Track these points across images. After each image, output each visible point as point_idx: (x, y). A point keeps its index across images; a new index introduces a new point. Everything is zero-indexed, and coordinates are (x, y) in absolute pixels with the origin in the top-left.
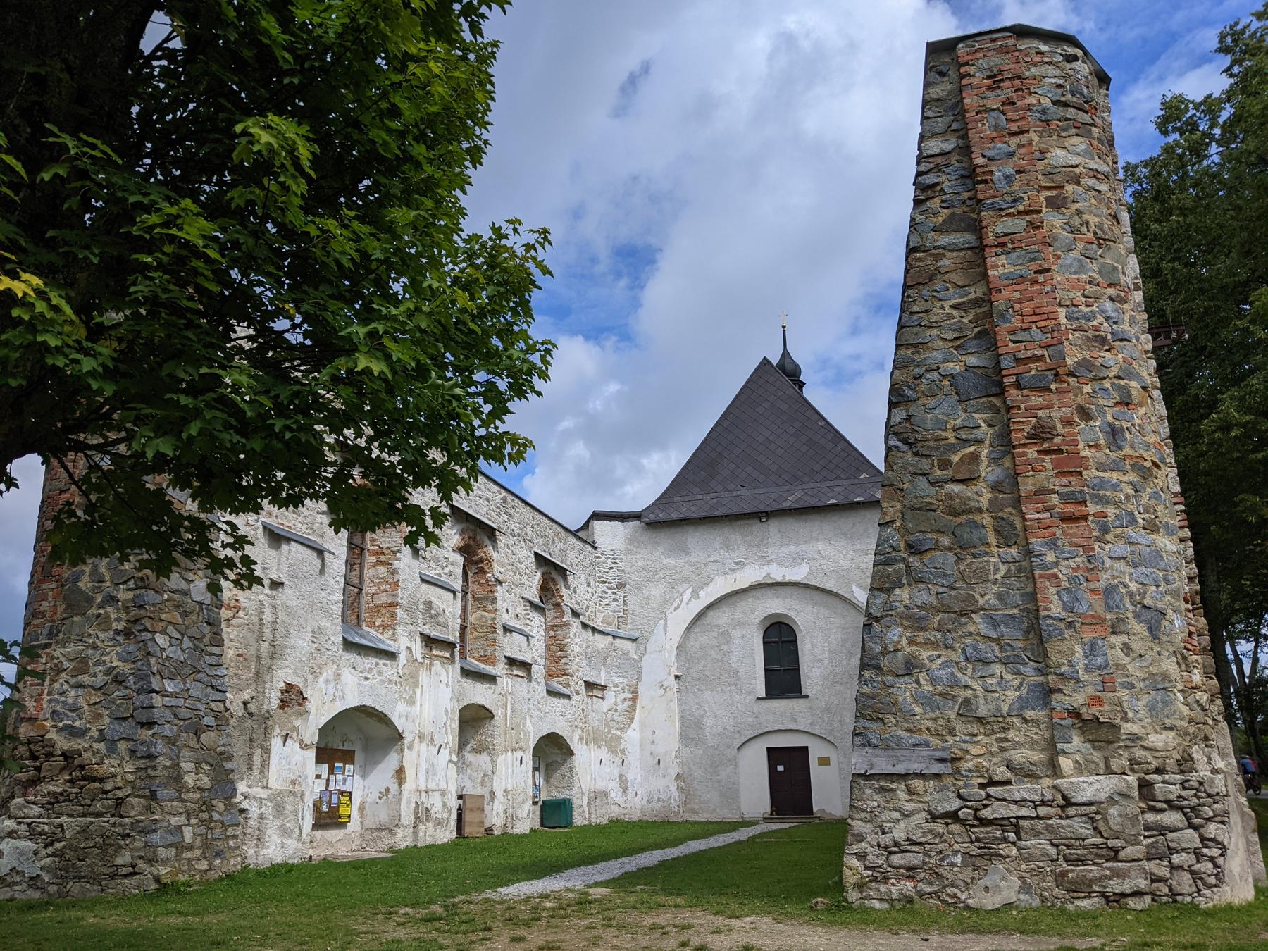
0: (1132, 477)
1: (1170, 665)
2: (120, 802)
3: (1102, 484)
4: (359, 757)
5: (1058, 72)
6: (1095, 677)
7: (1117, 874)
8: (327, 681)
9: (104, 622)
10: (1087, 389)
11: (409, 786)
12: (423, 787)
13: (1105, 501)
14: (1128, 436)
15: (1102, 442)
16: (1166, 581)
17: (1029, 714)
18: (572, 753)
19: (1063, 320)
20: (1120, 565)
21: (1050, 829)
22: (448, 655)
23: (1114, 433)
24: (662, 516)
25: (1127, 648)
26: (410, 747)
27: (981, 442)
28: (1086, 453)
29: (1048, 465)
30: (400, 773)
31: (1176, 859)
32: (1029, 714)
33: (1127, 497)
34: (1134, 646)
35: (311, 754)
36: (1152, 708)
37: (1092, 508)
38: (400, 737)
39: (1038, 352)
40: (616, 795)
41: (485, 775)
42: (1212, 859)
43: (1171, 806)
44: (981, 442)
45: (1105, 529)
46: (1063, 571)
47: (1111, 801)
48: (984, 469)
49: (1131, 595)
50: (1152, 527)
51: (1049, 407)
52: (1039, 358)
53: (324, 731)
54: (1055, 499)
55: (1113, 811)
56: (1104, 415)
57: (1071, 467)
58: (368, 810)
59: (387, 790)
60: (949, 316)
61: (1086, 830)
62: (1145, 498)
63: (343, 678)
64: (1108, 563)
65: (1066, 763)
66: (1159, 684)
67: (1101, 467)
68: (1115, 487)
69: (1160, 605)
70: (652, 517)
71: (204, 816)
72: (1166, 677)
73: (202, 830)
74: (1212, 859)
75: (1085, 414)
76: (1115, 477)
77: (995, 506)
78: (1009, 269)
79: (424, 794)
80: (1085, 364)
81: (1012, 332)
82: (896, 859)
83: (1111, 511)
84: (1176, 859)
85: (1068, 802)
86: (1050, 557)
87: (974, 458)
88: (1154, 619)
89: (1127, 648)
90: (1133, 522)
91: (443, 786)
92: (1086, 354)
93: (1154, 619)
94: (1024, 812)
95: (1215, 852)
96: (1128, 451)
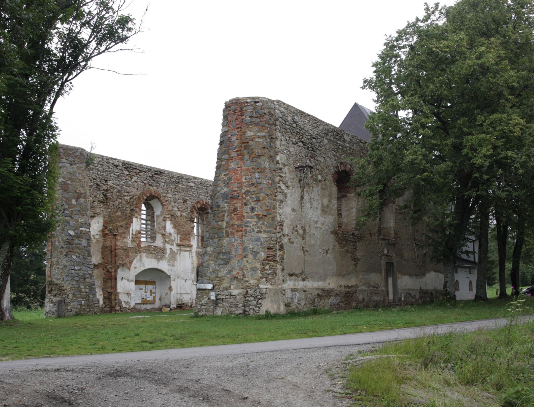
0: (256, 220)
1: (258, 265)
2: (68, 295)
3: (247, 222)
5: (251, 108)
6: (238, 268)
7: (237, 310)
8: (137, 261)
9: (61, 252)
10: (248, 198)
11: (173, 292)
12: (179, 292)
13: (247, 226)
14: (257, 209)
15: (249, 211)
16: (261, 245)
17: (228, 276)
19: (243, 180)
20: (248, 242)
21: (228, 301)
23: (253, 209)
25: (247, 261)
27: (225, 211)
28: (245, 214)
29: (235, 218)
30: (170, 288)
31: (251, 307)
32: (228, 276)
33: (253, 225)
34: (249, 261)
35: (134, 283)
36: (252, 274)
37: (244, 228)
38: (169, 277)
39: (236, 189)
42: (259, 307)
43: (252, 296)
44: (225, 211)
45: (246, 233)
46: (235, 244)
47: (238, 295)
48: (225, 218)
49: (250, 249)
50: (260, 232)
51: (237, 203)
52: (237, 191)
54: (236, 226)
55: (238, 297)
56: (251, 204)
57: (241, 217)
58: (162, 300)
60: (223, 178)
61: (233, 301)
62: (259, 225)
64: (246, 241)
65: (232, 287)
66: (254, 269)
67: (248, 218)
68: (251, 222)
69: (258, 251)
71: (87, 298)
72: (256, 267)
73: (87, 302)
74: (259, 307)
75: (246, 204)
76: (251, 220)
77: (226, 227)
78: (233, 166)
79: (179, 295)
80: (248, 191)
81: (232, 183)
82: (202, 307)
83: (248, 229)
84: (251, 307)
85: (231, 295)
86: (233, 241)
87: (224, 216)
88: (256, 254)
89: (247, 261)
90: (253, 231)
92: (248, 189)
93: (256, 254)
94: (224, 297)
95: (260, 306)
96: (256, 213)
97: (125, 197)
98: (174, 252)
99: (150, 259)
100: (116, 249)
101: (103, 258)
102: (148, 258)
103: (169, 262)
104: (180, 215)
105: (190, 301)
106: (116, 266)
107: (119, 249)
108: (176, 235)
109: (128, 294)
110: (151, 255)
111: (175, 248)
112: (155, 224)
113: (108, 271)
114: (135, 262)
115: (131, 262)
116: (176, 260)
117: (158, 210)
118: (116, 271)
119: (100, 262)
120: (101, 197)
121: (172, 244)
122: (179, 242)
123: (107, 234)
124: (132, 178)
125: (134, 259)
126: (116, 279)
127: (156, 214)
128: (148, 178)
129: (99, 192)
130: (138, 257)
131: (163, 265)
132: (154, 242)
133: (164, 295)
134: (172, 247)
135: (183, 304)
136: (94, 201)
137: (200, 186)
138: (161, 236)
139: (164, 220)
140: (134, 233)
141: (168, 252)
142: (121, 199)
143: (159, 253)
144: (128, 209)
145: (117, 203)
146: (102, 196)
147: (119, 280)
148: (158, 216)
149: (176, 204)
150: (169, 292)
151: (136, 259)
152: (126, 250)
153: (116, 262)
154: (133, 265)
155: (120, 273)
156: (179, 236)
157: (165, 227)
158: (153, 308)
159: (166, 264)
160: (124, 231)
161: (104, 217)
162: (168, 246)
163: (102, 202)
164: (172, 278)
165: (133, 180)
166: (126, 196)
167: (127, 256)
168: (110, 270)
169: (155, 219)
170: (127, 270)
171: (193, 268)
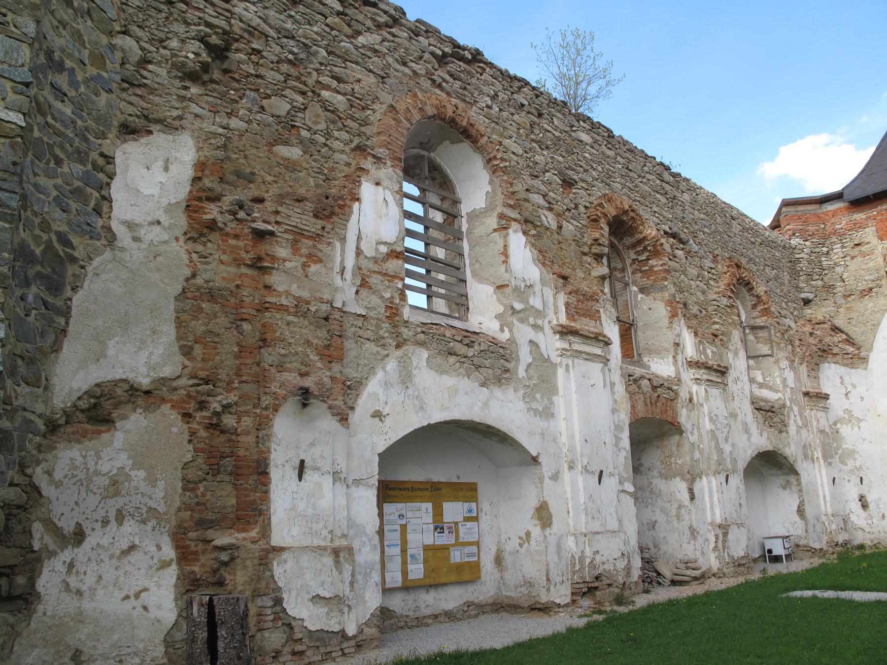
4: (482, 491)
8: (387, 385)
18: (796, 473)
22: (598, 351)
24: (871, 190)
26: (555, 477)
30: (543, 515)
40: (858, 517)
41: (680, 507)
53: (387, 457)
58: (508, 560)
59: (528, 534)
63: (416, 380)
70: (859, 194)
91: (613, 524)
97: (325, 94)
98: (548, 360)
99: (449, 381)
100: (263, 308)
101: (187, 351)
102: (441, 371)
103: (528, 397)
104: (554, 226)
105: (621, 564)
106: (266, 400)
107: (282, 308)
108: (549, 293)
109: (336, 552)
110: (452, 359)
111: (552, 345)
112: (465, 245)
113: (214, 426)
114: (373, 386)
115: (351, 388)
116: (554, 391)
117: (476, 190)
118: (263, 424)
119: (167, 371)
120: (192, 53)
121: (537, 327)
122: (563, 319)
123: (212, 226)
124: (359, 33)
125: (372, 371)
126: (261, 471)
127: (465, 208)
128: (427, 56)
129: (180, 28)
130: (391, 365)
131: (504, 410)
132: (463, 318)
133: (515, 543)
134: (539, 338)
135: (597, 578)
136: (145, 62)
137: (609, 152)
138: (491, 289)
139: (503, 228)
140: (368, 250)
141: (525, 356)
142: (303, 93)
143: (489, 360)
144: (336, 145)
145: (281, 107)
146: (196, 45)
147: (281, 480)
148: (474, 216)
149: (537, 183)
150: (536, 532)
151: (380, 374)
152: (331, 320)
153: (261, 379)
154: (365, 403)
155: (289, 436)
156: (562, 298)
157: (505, 253)
158: (469, 604)
159: (521, 405)
160: (312, 225)
161: (204, 139)
162: (524, 333)
163: (192, 77)
164: (547, 468)
165: (361, 40)
166: (327, 87)
167: (331, 353)
168: (229, 421)
169: (464, 228)
170: (328, 423)
171: (618, 428)
